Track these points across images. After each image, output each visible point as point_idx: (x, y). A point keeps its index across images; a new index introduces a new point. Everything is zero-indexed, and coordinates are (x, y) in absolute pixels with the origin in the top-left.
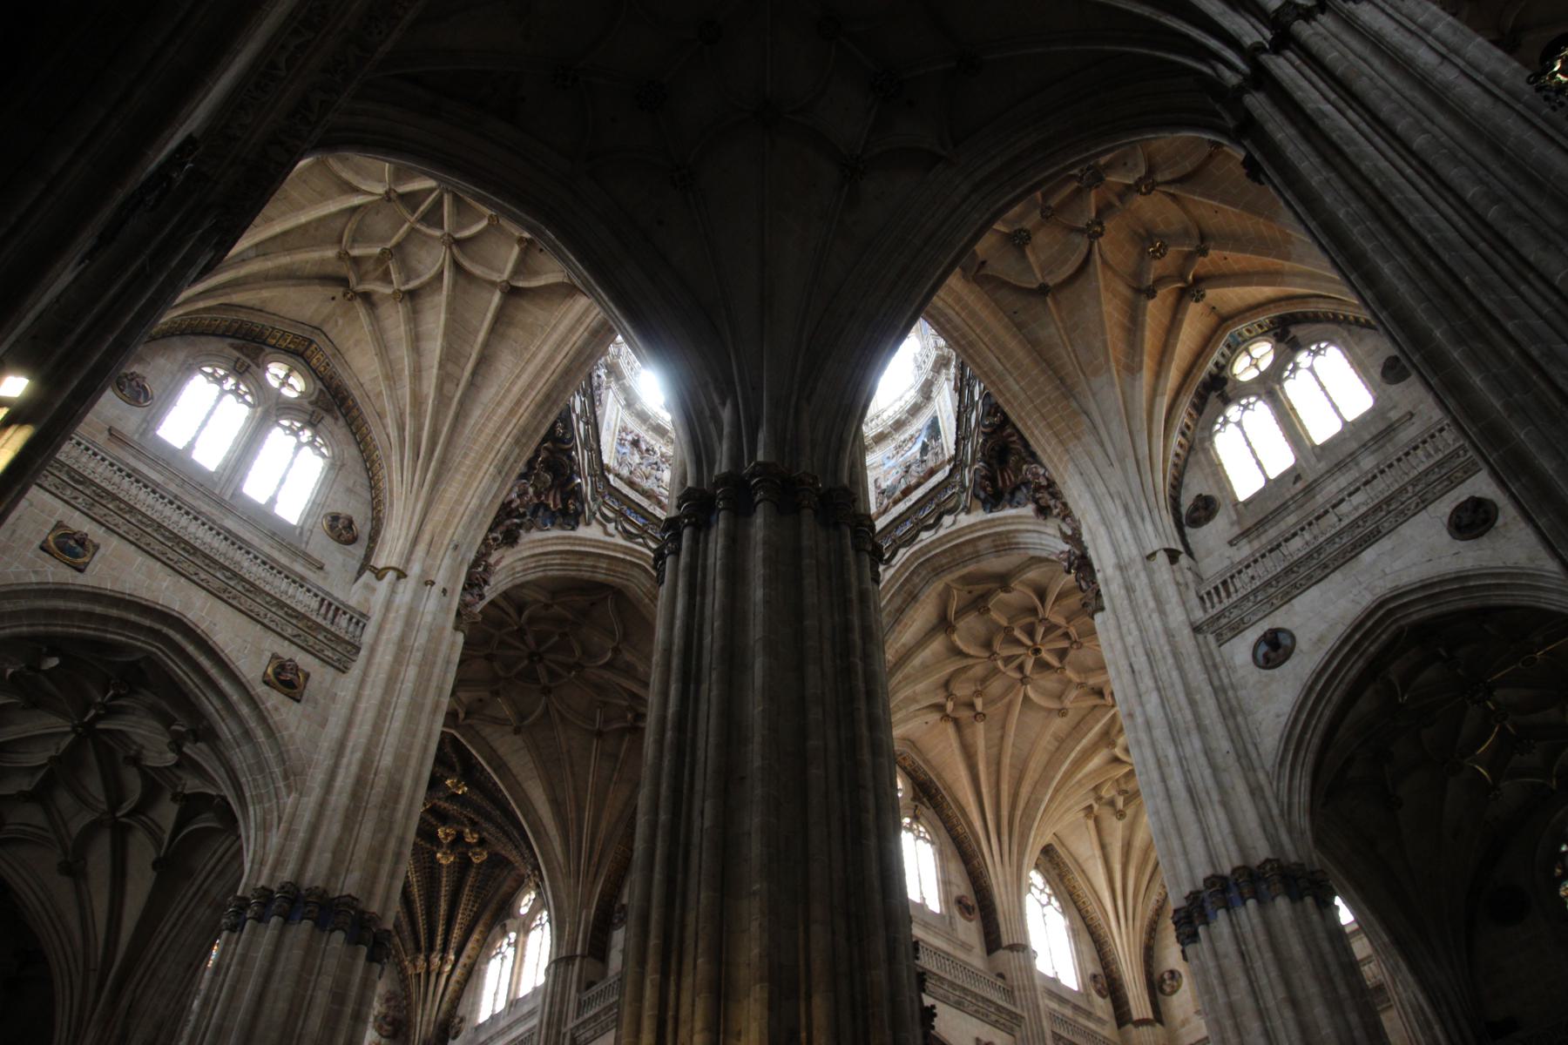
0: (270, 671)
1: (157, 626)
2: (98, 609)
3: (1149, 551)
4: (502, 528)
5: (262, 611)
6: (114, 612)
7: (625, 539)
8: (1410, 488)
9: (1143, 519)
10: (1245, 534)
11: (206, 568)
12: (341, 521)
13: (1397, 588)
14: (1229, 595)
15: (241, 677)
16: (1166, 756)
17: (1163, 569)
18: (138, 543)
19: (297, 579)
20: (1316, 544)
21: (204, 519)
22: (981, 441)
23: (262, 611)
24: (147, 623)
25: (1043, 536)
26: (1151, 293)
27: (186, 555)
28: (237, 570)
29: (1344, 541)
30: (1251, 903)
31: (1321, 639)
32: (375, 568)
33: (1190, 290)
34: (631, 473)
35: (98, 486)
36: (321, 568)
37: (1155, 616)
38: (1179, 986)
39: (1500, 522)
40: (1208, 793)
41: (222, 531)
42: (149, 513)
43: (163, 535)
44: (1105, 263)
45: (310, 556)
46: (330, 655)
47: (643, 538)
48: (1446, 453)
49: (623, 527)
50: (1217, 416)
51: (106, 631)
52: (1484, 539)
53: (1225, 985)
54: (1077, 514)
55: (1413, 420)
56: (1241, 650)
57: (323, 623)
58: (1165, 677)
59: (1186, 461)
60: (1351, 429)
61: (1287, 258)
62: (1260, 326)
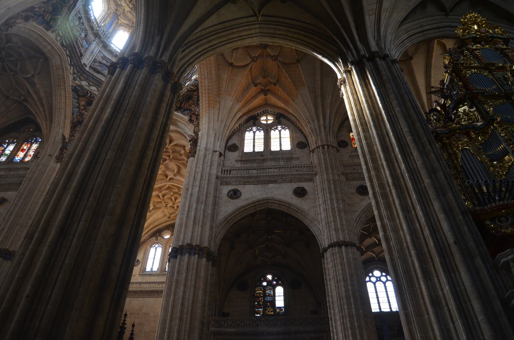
3: (215, 150)
4: (26, 13)
7: (61, 45)
8: (290, 176)
9: (218, 140)
10: (241, 161)
13: (273, 197)
14: (230, 174)
16: (192, 206)
17: (217, 157)
20: (260, 175)
22: (185, 91)
25: (186, 127)
26: (256, 85)
29: (267, 178)
30: (196, 256)
31: (248, 199)
33: (265, 92)
34: (74, 26)
37: (208, 167)
38: (138, 265)
39: (305, 197)
40: (199, 221)
44: (251, 69)
47: (66, 49)
48: (303, 173)
49: (62, 41)
50: (250, 127)
52: (300, 198)
53: (178, 274)
54: (201, 128)
55: (298, 160)
56: (226, 190)
58: (203, 185)
59: (236, 132)
60: (281, 152)
61: (294, 101)
62: (274, 112)
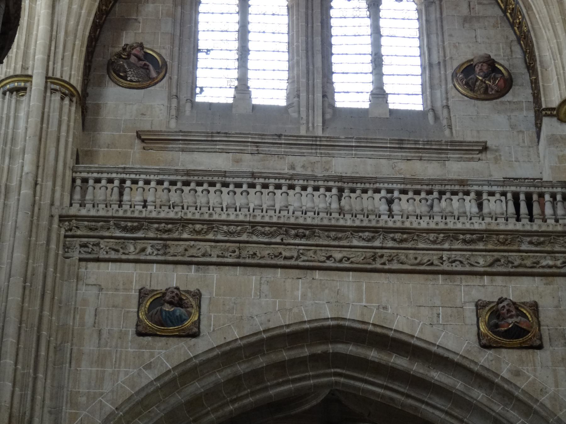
0: (483, 328)
1: (319, 349)
2: (242, 368)
5: (434, 257)
6: (261, 361)
11: (336, 243)
12: (477, 70)
15: (451, 356)
18: (241, 261)
19: (457, 187)
21: (301, 182)
23: (434, 257)
24: (306, 352)
27: (303, 241)
28: (373, 224)
32: (553, 109)
35: (159, 221)
36: (485, 148)
41: (331, 184)
42: (232, 218)
43: (264, 234)
45: (461, 143)
46: (551, 263)
51: (266, 389)
57: (519, 226)
